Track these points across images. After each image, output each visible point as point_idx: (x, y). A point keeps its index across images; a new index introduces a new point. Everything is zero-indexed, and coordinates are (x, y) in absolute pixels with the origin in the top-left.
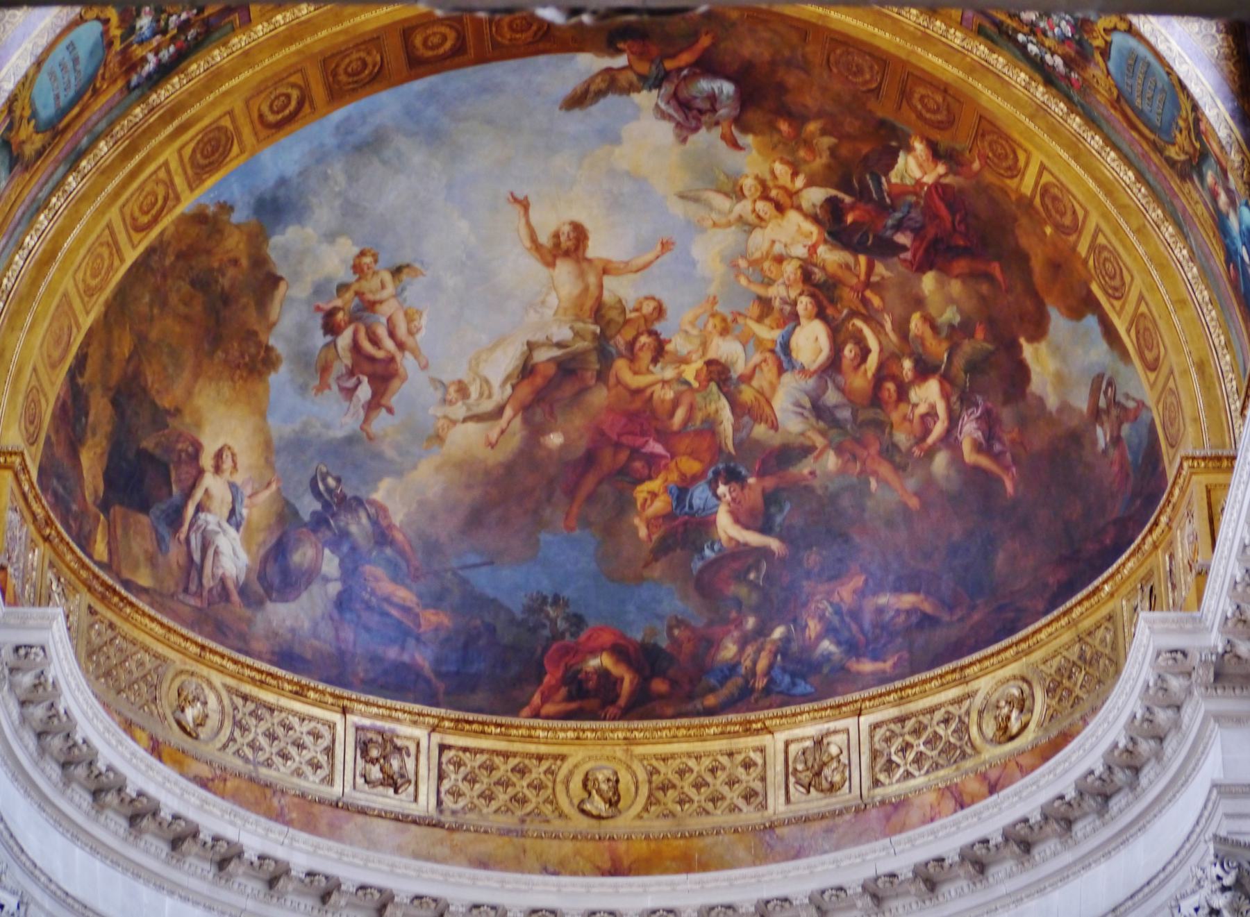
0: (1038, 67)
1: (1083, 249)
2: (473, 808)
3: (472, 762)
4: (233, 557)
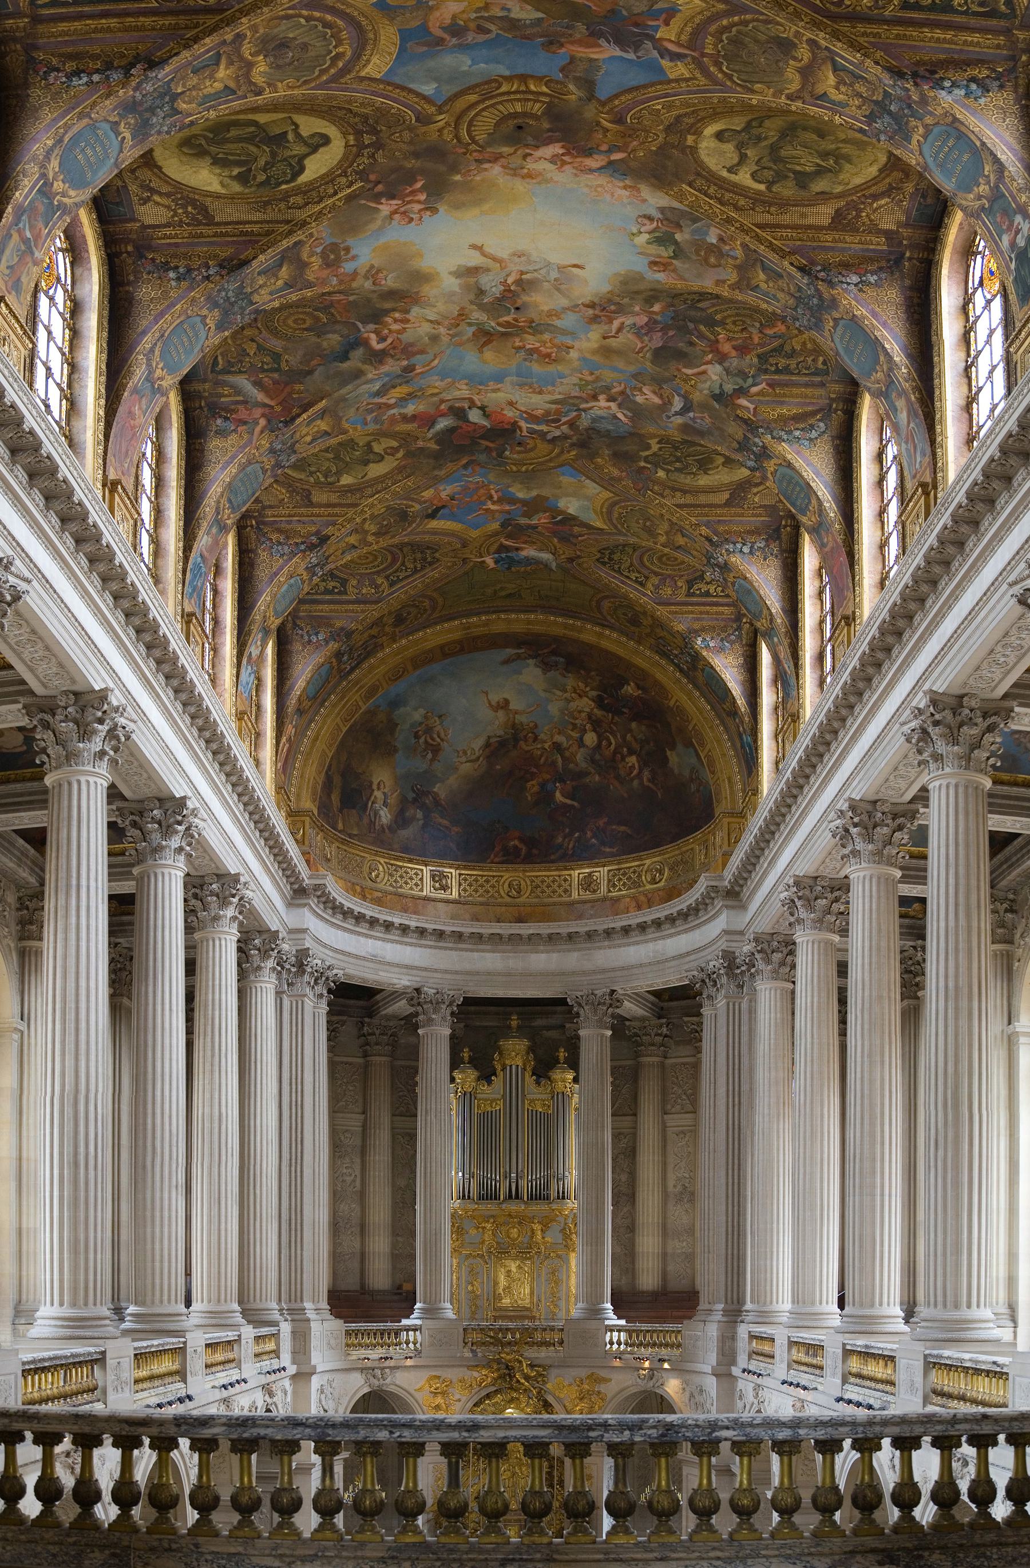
0: (677, 666)
1: (690, 728)
2: (471, 895)
3: (470, 879)
4: (385, 816)
